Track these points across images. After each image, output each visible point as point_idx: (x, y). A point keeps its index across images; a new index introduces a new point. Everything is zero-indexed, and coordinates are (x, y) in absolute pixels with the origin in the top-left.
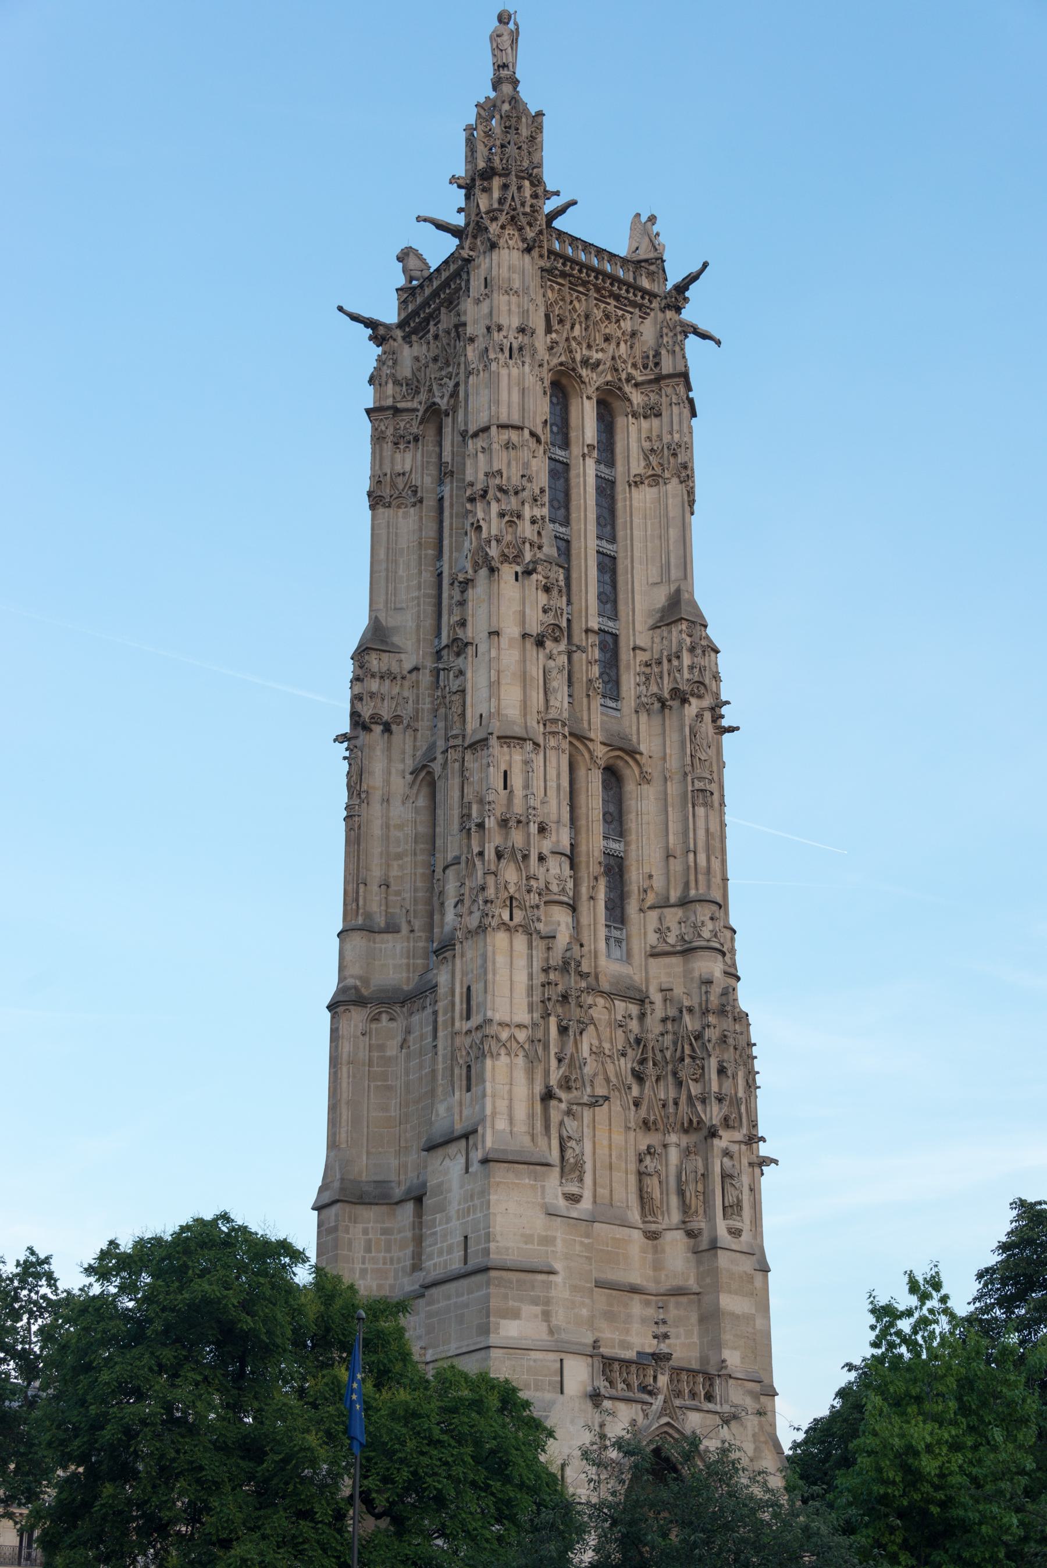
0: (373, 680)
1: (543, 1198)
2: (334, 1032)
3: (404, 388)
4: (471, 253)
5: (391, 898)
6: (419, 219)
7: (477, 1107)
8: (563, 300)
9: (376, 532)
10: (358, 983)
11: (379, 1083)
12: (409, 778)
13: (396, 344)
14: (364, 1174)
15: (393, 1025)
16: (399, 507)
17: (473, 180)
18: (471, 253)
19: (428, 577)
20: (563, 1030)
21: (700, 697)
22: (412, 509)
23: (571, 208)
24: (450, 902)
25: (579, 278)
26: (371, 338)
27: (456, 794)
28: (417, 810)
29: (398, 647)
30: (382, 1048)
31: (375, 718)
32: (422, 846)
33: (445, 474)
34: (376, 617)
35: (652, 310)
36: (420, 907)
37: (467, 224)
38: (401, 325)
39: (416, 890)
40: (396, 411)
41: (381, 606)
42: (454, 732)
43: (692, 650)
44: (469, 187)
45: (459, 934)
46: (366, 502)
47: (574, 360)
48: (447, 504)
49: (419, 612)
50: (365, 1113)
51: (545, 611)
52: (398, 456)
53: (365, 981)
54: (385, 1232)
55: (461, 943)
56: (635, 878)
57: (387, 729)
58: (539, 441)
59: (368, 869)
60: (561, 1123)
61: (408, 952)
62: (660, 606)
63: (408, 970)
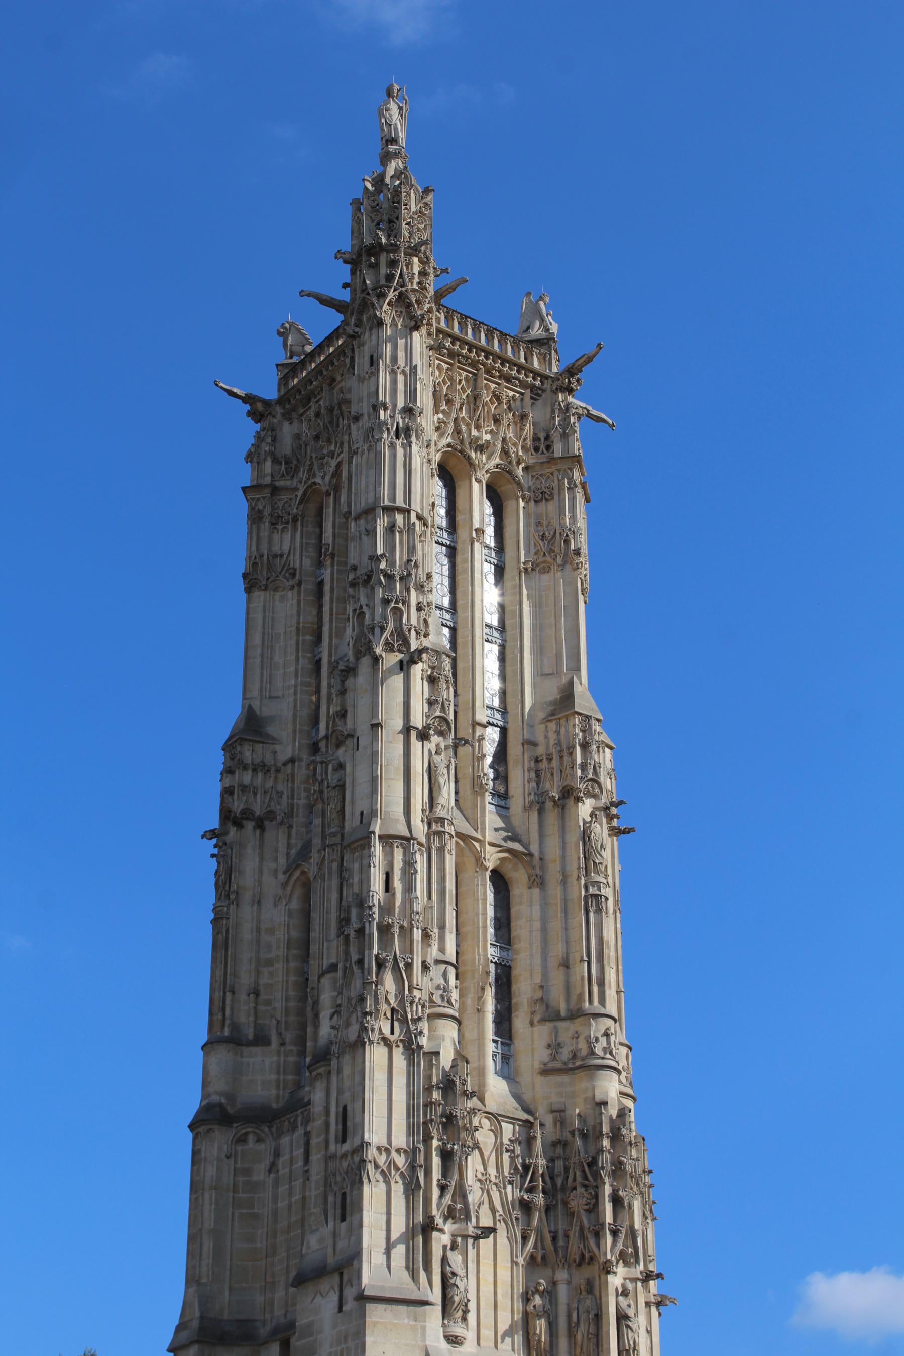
0: (245, 773)
1: (424, 1341)
2: (195, 1153)
3: (283, 467)
4: (357, 330)
5: (261, 1008)
6: (302, 294)
7: (353, 1238)
8: (451, 379)
9: (251, 616)
10: (223, 1101)
11: (244, 1211)
12: (282, 877)
13: (275, 421)
14: (226, 1312)
15: (261, 1146)
16: (276, 589)
17: (359, 255)
18: (357, 330)
19: (305, 663)
20: (447, 1156)
21: (595, 796)
22: (290, 594)
23: (462, 287)
24: (325, 1015)
25: (467, 358)
26: (249, 414)
27: (335, 896)
28: (290, 914)
29: (273, 738)
30: (247, 1172)
31: (247, 814)
32: (295, 952)
34: (250, 706)
35: (544, 391)
36: (292, 1018)
37: (353, 300)
38: (281, 401)
39: (287, 1000)
40: (275, 490)
41: (255, 693)
42: (333, 830)
43: (585, 746)
44: (354, 262)
45: (335, 1048)
46: (240, 584)
47: (462, 442)
48: (327, 588)
49: (295, 701)
50: (229, 1243)
51: (431, 703)
52: (276, 537)
55: (338, 1058)
56: (524, 989)
57: (260, 825)
58: (425, 525)
59: (235, 975)
60: (444, 1260)
61: (278, 1067)
62: (551, 698)
63: (278, 1087)
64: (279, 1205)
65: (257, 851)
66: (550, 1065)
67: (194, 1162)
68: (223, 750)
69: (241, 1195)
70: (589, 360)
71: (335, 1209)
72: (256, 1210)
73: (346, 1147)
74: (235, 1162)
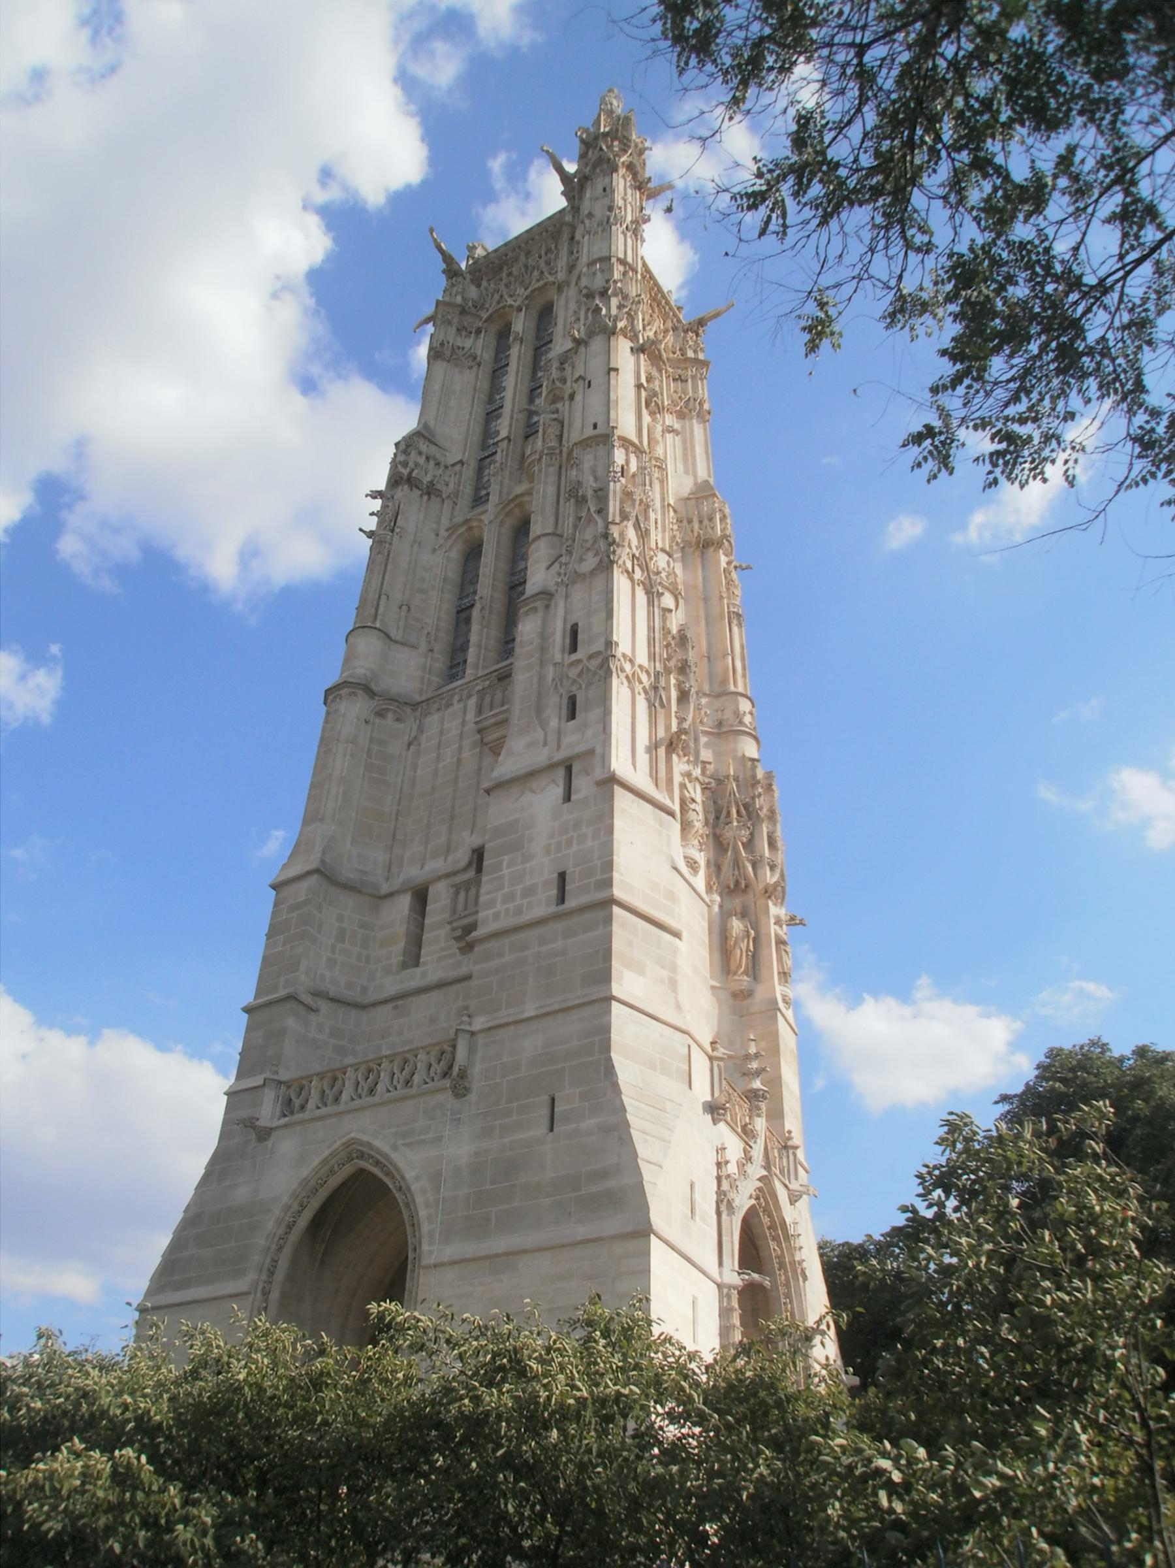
16: (457, 365)
33: (514, 340)
39: (439, 619)
54: (362, 925)
64: (419, 772)
67: (326, 721)
68: (397, 445)
70: (717, 315)
73: (575, 657)
74: (372, 731)
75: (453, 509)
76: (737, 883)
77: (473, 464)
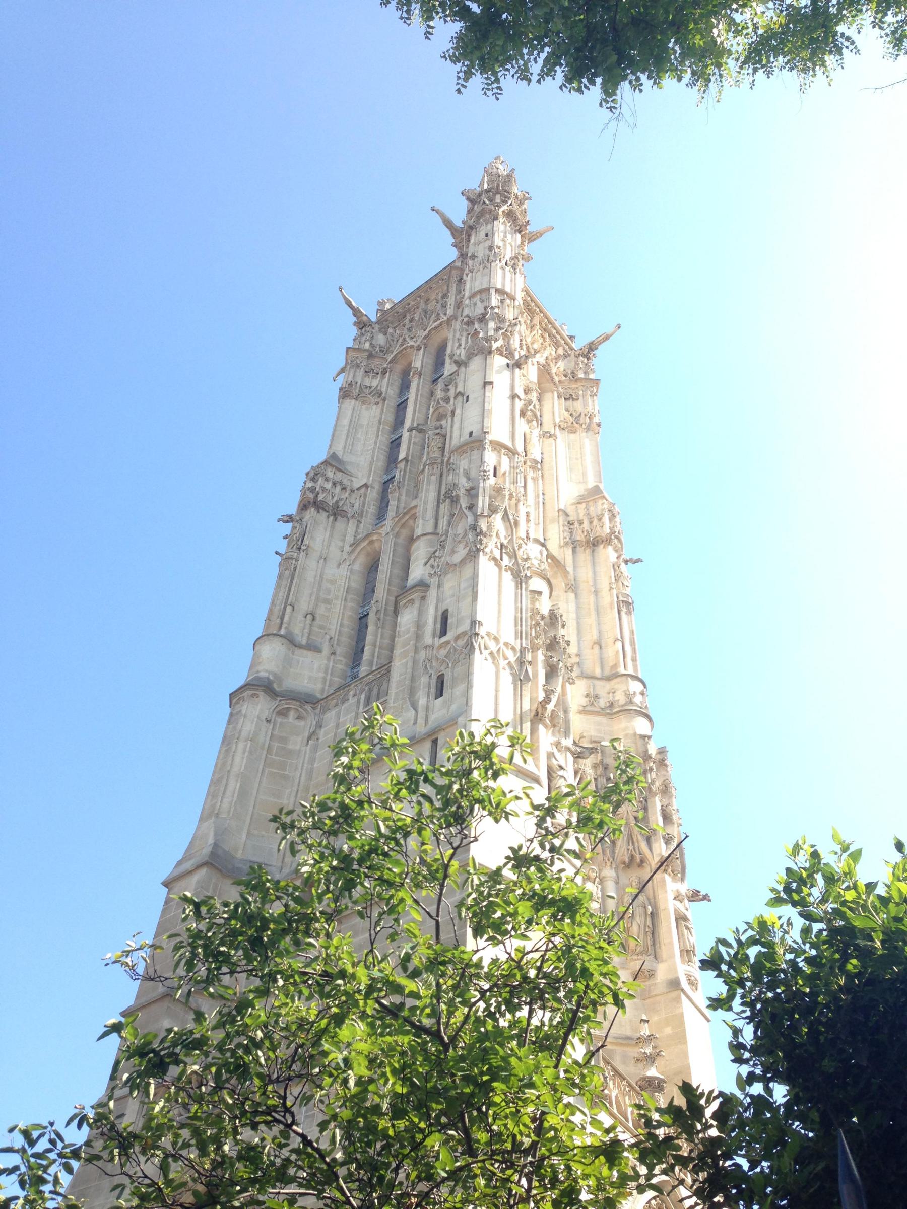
5: (315, 629)
14: (240, 852)
15: (302, 723)
16: (364, 402)
19: (384, 439)
22: (375, 406)
30: (283, 740)
36: (344, 639)
50: (255, 792)
53: (279, 679)
65: (329, 529)
66: (589, 708)
67: (229, 723)
69: (273, 757)
70: (607, 338)
71: (429, 688)
72: (286, 773)
73: (444, 639)
75: (358, 527)
76: (632, 858)
77: (377, 486)
